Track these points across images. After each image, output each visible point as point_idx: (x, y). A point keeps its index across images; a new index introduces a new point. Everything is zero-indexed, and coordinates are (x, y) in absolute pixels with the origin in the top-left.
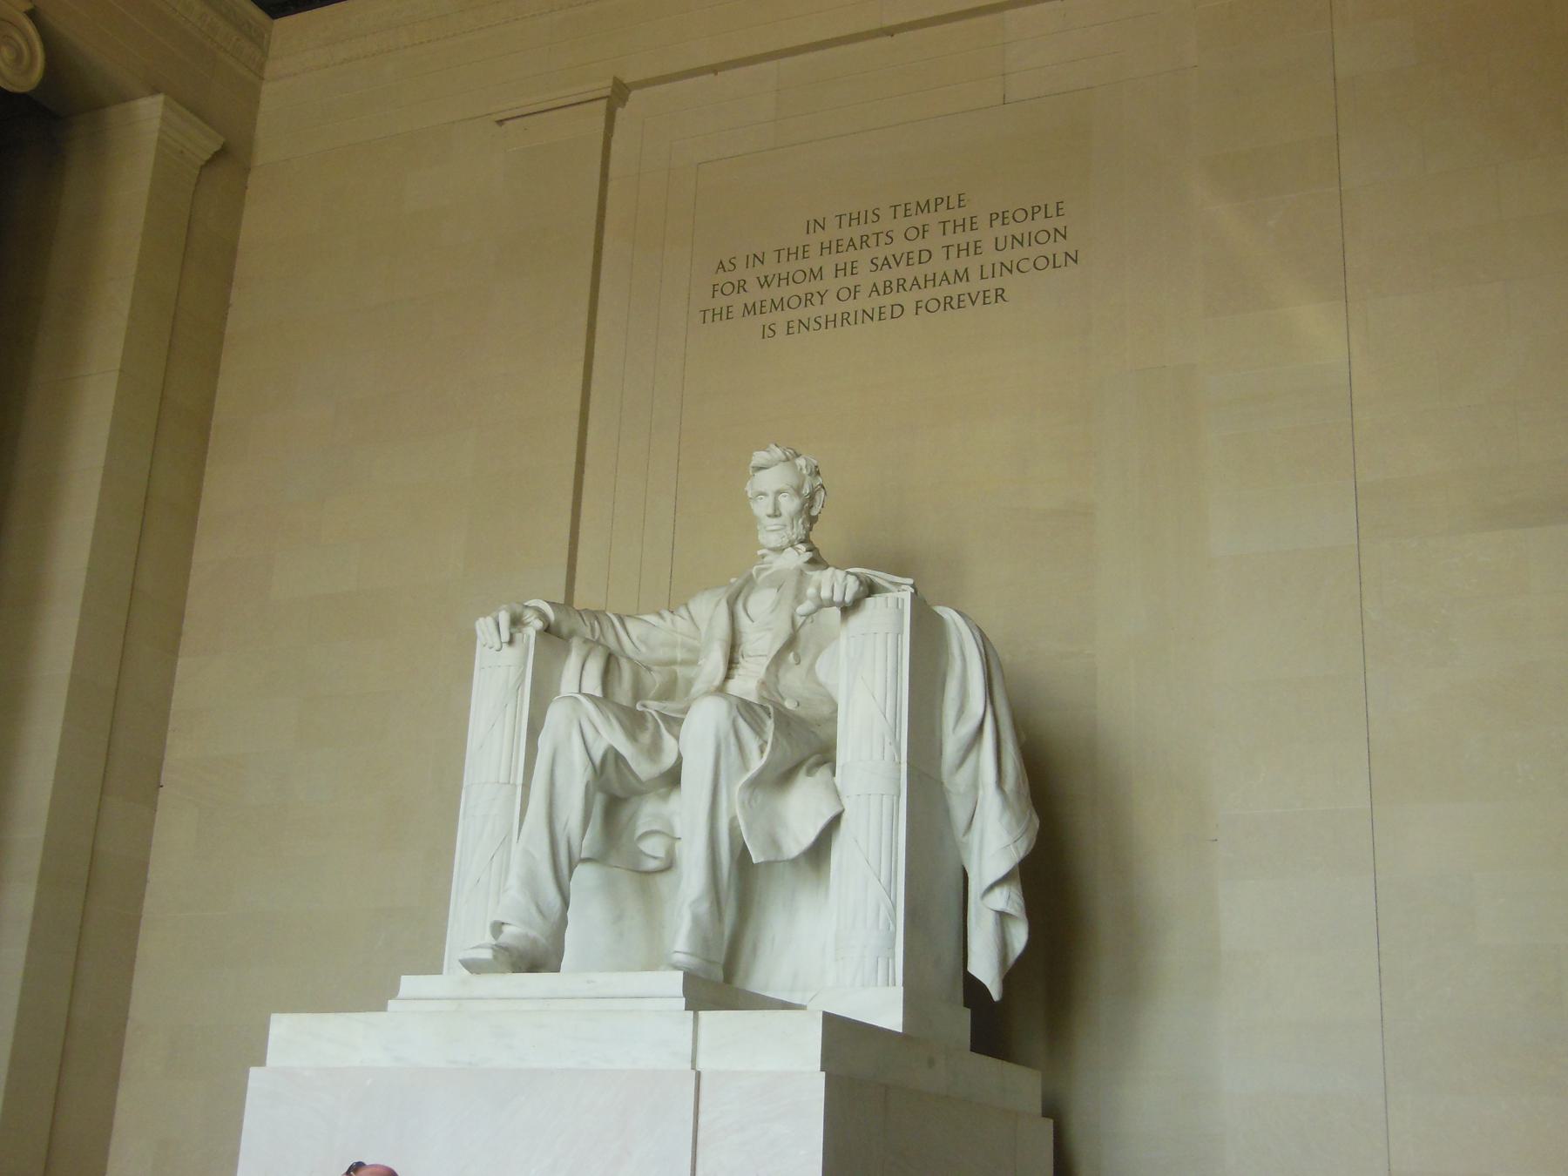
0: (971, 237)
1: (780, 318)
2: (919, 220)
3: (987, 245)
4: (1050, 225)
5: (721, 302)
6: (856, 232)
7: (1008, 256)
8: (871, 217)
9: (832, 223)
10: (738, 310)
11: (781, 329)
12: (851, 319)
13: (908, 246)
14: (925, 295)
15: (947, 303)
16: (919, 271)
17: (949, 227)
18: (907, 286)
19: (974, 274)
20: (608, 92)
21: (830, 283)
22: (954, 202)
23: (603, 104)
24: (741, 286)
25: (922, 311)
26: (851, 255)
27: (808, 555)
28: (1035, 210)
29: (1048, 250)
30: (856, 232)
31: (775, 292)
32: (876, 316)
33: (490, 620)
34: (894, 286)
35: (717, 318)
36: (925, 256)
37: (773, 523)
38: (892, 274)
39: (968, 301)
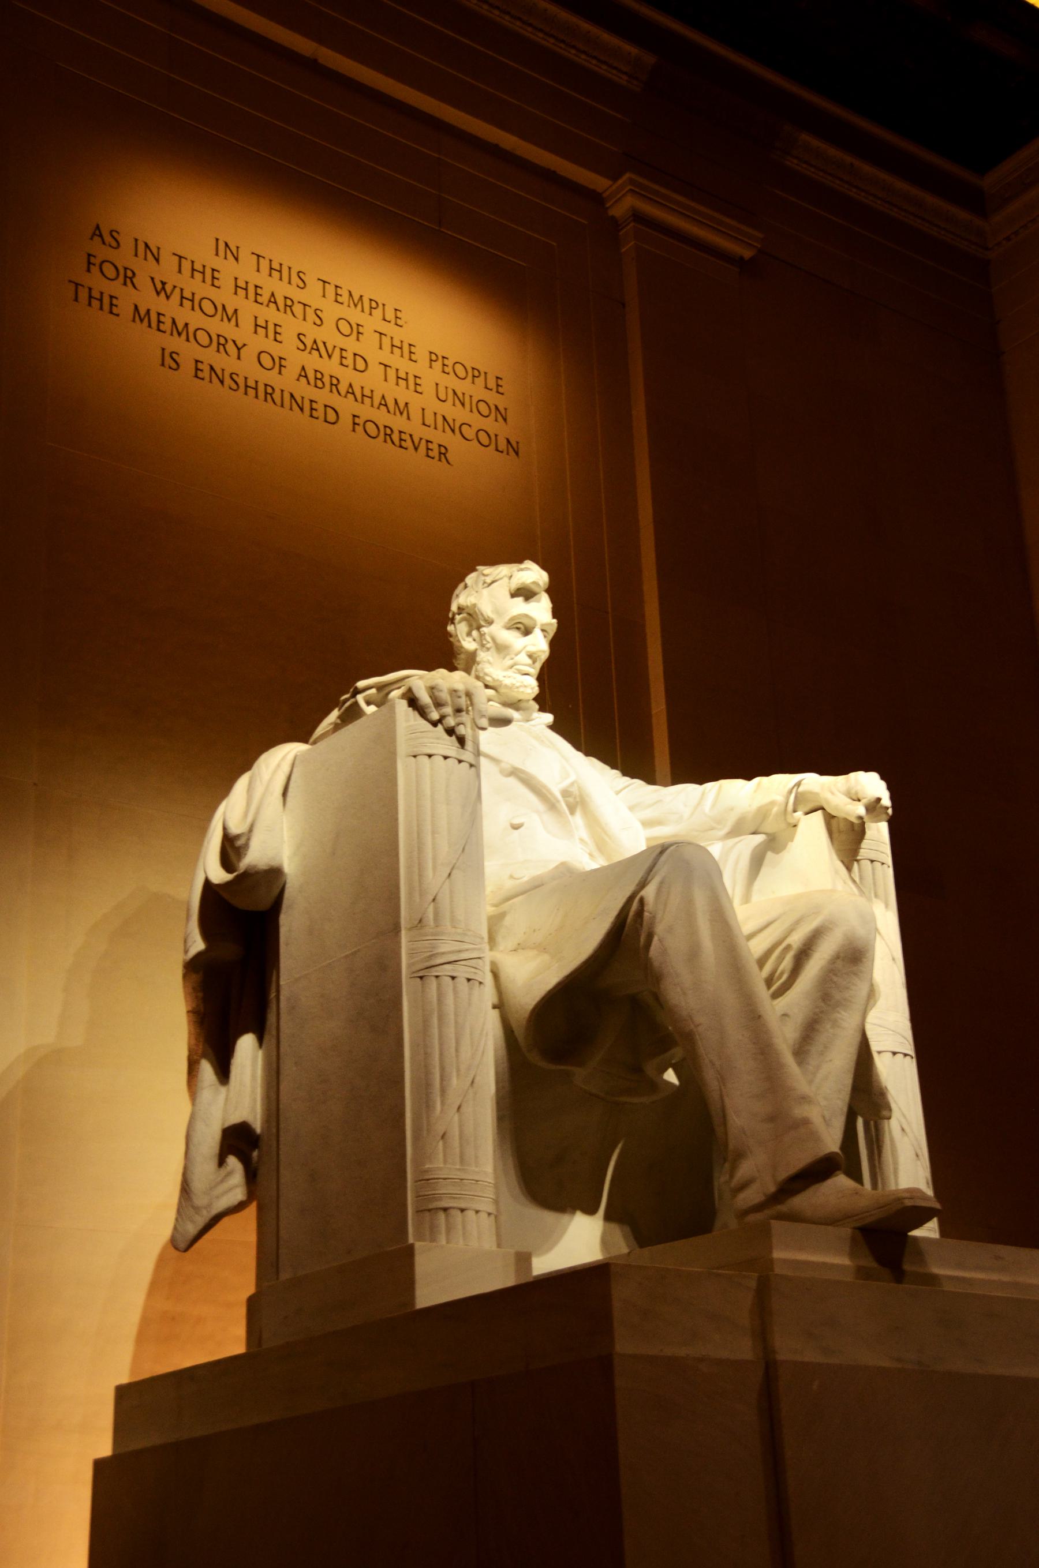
0: (413, 369)
2: (355, 315)
4: (492, 398)
5: (96, 282)
8: (295, 279)
9: (247, 260)
10: (125, 308)
11: (188, 367)
12: (277, 396)
13: (341, 342)
16: (358, 381)
18: (343, 388)
22: (390, 315)
24: (129, 278)
25: (359, 429)
26: (270, 314)
27: (549, 718)
28: (476, 374)
29: (491, 425)
30: (282, 289)
32: (307, 408)
34: (326, 380)
35: (96, 304)
36: (361, 365)
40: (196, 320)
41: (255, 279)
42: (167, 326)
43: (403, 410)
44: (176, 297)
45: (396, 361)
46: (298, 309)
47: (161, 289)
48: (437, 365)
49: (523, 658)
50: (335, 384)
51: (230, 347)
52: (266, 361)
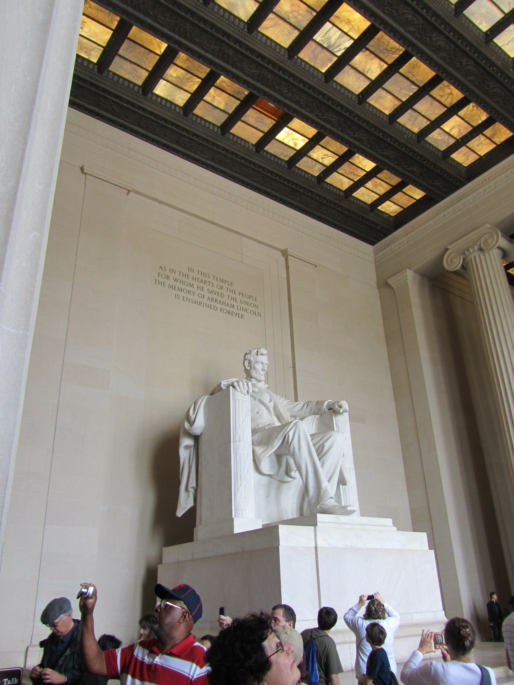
0: (235, 296)
1: (181, 294)
3: (239, 301)
4: (254, 303)
6: (204, 279)
7: (245, 306)
8: (207, 276)
10: (167, 285)
11: (181, 298)
12: (202, 304)
13: (218, 290)
14: (223, 307)
15: (229, 312)
16: (222, 300)
17: (229, 290)
18: (218, 302)
19: (236, 307)
20: (131, 189)
21: (195, 289)
22: (230, 283)
23: (126, 191)
26: (201, 285)
27: (267, 386)
29: (254, 309)
30: (204, 279)
31: (178, 284)
33: (245, 384)
35: (160, 284)
36: (222, 296)
37: (263, 373)
38: (215, 297)
39: (234, 314)
40: (183, 287)
41: (198, 276)
42: (177, 289)
43: (233, 306)
44: (179, 282)
45: (231, 294)
46: (208, 283)
47: (176, 280)
48: (241, 295)
49: (260, 371)
50: (216, 301)
51: (192, 293)
52: (200, 296)
